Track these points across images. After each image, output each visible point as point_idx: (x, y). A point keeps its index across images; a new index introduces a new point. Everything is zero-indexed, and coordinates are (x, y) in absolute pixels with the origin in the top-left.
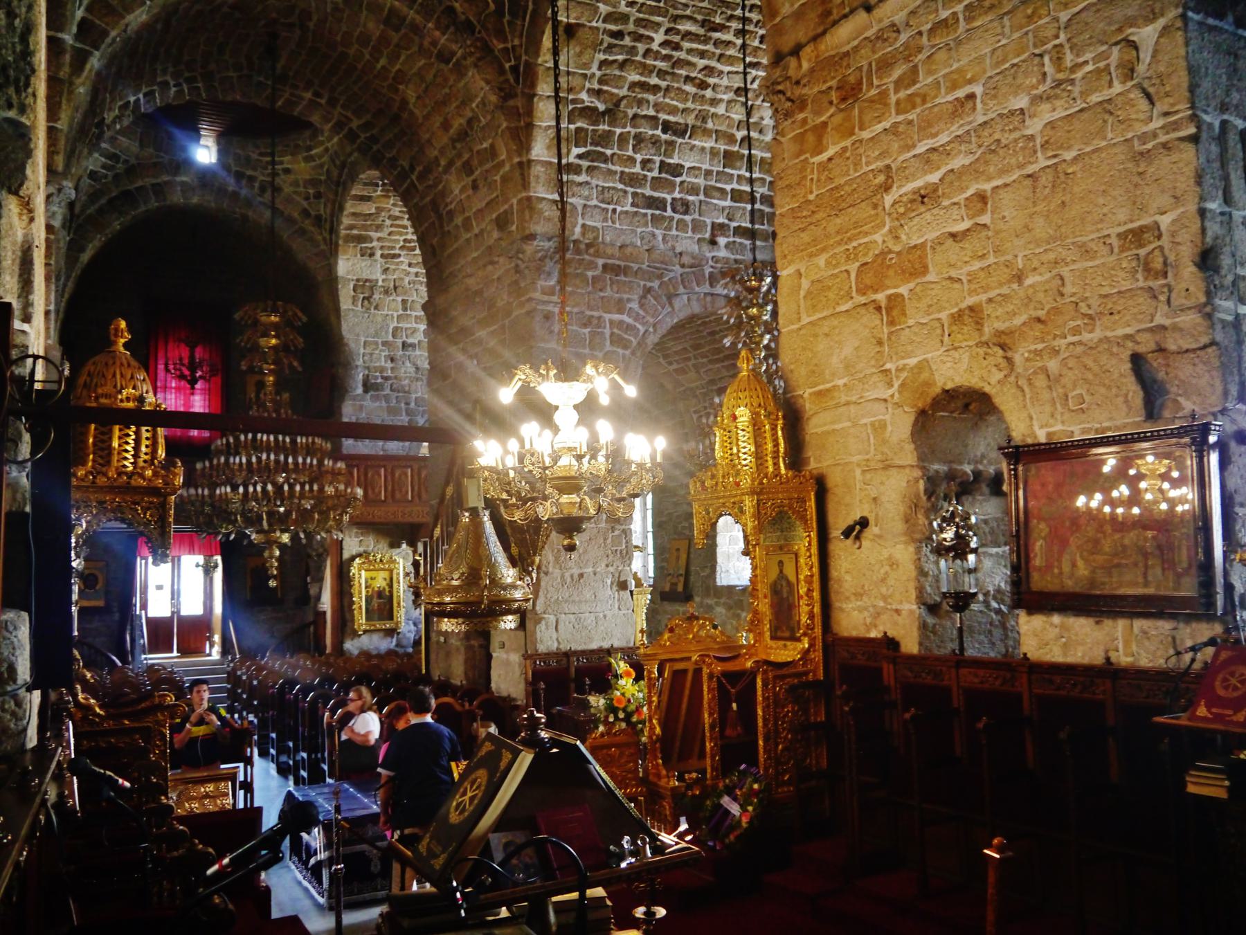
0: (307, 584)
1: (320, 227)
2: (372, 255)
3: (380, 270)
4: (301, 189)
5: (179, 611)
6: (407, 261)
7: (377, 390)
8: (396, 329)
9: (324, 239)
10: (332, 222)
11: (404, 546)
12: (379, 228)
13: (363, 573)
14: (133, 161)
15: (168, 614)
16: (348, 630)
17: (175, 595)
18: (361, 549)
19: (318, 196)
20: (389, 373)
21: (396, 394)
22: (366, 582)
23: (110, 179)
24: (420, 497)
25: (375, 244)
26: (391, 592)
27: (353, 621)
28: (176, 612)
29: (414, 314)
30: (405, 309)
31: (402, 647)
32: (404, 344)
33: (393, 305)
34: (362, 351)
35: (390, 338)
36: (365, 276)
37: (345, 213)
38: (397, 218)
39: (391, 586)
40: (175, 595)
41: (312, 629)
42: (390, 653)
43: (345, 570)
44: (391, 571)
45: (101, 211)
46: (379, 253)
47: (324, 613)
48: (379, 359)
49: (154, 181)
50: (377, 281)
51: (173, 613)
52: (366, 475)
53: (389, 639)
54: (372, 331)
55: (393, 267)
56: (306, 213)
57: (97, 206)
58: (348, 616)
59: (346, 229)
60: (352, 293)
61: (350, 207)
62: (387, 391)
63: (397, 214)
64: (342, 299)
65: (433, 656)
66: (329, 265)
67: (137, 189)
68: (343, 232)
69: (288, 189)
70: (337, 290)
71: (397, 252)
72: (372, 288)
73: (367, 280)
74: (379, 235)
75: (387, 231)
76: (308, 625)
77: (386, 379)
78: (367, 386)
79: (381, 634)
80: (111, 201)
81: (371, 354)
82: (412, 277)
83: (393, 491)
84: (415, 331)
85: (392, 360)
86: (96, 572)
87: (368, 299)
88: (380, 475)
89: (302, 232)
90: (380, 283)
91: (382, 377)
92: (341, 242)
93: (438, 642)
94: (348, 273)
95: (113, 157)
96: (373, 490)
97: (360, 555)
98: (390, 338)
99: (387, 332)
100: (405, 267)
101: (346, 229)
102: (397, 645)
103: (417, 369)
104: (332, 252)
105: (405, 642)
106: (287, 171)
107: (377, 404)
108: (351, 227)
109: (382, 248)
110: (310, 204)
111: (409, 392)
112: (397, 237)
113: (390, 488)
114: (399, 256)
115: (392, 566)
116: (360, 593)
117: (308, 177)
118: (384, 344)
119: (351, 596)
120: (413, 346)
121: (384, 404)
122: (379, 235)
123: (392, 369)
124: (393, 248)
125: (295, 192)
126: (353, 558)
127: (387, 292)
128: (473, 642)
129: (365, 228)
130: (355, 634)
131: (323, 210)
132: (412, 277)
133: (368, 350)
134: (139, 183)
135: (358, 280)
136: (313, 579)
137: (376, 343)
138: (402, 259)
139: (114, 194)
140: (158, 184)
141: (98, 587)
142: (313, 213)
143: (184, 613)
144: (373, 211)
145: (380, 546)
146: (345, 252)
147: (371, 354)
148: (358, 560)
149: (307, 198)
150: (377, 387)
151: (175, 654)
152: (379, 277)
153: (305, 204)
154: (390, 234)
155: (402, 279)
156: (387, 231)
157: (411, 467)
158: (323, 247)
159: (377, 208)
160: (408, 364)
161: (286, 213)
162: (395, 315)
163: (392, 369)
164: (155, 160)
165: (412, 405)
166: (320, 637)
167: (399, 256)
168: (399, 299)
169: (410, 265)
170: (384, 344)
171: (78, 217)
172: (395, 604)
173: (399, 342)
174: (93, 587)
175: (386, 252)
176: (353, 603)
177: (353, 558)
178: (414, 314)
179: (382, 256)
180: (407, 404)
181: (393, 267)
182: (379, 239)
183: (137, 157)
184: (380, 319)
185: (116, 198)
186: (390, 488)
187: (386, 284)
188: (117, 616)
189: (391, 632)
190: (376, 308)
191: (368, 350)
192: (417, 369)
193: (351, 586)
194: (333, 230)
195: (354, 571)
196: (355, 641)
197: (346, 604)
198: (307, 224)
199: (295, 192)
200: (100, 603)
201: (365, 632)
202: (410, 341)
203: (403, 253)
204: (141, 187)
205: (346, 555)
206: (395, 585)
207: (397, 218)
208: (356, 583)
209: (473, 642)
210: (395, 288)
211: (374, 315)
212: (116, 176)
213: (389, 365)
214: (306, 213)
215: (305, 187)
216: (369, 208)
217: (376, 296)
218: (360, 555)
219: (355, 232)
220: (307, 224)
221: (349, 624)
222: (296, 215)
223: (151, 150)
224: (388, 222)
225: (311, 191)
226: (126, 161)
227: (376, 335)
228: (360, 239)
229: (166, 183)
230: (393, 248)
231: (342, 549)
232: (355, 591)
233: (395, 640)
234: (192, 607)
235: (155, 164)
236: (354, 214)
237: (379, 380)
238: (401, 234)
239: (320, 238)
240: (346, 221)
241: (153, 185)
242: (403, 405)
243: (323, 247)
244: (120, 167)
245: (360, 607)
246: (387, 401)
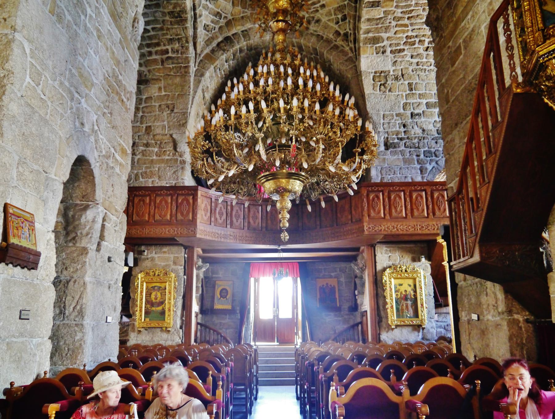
0: (355, 296)
1: (347, 41)
2: (383, 52)
3: (391, 63)
4: (333, 17)
5: (278, 316)
6: (410, 54)
7: (395, 147)
8: (405, 105)
9: (351, 49)
10: (355, 34)
11: (423, 260)
12: (387, 29)
13: (393, 280)
14: (230, 17)
15: (271, 317)
16: (384, 324)
17: (276, 306)
18: (390, 263)
19: (344, 18)
20: (403, 135)
21: (408, 150)
22: (395, 287)
23: (217, 29)
24: (434, 214)
25: (386, 43)
26: (415, 296)
27: (387, 317)
28: (276, 316)
29: (418, 92)
30: (411, 90)
31: (427, 340)
32: (412, 114)
33: (402, 88)
34: (382, 121)
35: (402, 111)
36: (380, 69)
37: (363, 19)
38: (400, 19)
39: (415, 291)
40: (276, 306)
41: (360, 326)
42: (418, 344)
43: (379, 278)
44: (415, 279)
45: (213, 51)
46: (389, 50)
47: (366, 311)
48: (395, 126)
49: (244, 29)
50: (389, 71)
51: (274, 316)
52: (389, 198)
53: (416, 333)
54: (388, 107)
55: (400, 60)
56: (338, 33)
57: (210, 48)
58: (382, 313)
59: (365, 33)
60: (373, 82)
61: (366, 13)
62: (403, 148)
63: (400, 15)
64: (365, 87)
65: (464, 338)
66: (355, 66)
67: (233, 35)
68: (362, 36)
69: (324, 19)
70: (362, 80)
71: (402, 47)
72: (386, 77)
73: (381, 72)
74: (388, 35)
75: (393, 30)
76: (357, 325)
77: (401, 139)
78: (387, 146)
79: (410, 329)
80: (218, 44)
81: (389, 123)
82: (414, 66)
83: (412, 210)
84: (419, 104)
85: (404, 126)
86: (226, 287)
87: (384, 85)
88: (400, 198)
89: (336, 47)
90: (392, 73)
91: (398, 139)
92: (361, 45)
93: (469, 321)
94: (368, 68)
95: (218, 14)
96: (396, 208)
97: (390, 267)
98: (402, 111)
99: (399, 107)
100: (408, 58)
101: (365, 33)
102: (423, 339)
103: (424, 130)
104: (356, 52)
105: (429, 336)
106: (323, 6)
107: (396, 157)
108: (368, 32)
109: (391, 45)
110: (339, 26)
111: (419, 147)
112: (401, 35)
113: (409, 207)
114: (404, 50)
115: (415, 275)
116: (391, 296)
117: (336, 6)
118: (397, 115)
119: (385, 297)
120: (419, 115)
121: (400, 157)
122: (388, 35)
123: (405, 132)
124: (398, 44)
125: (329, 20)
126: (384, 270)
127: (396, 78)
128: (516, 316)
129: (377, 30)
130: (389, 328)
131: (347, 28)
132: (414, 66)
133: (386, 120)
134: (234, 31)
135: (376, 73)
136: (359, 292)
137: (392, 115)
138: (405, 53)
139: (220, 39)
140: (246, 31)
141: (227, 297)
142: (342, 33)
143: (281, 316)
144: (382, 15)
145: (405, 260)
146: (365, 51)
147: (389, 123)
148: (388, 269)
149: (337, 23)
150: (395, 146)
151: (276, 343)
152: (389, 67)
153: (336, 27)
154: (395, 33)
155: (408, 68)
156: (393, 30)
157: (425, 190)
158: (351, 55)
159: (385, 12)
160: (416, 127)
161: (325, 37)
162: (404, 94)
163: (405, 132)
164: (242, 15)
165: (422, 156)
166: (364, 334)
167: (404, 50)
168: (406, 82)
169: (412, 57)
170: (397, 115)
171: (200, 55)
172: (419, 305)
173: (408, 113)
174: (225, 297)
175: (394, 48)
176: (385, 303)
177: (384, 270)
178: (418, 92)
179: (391, 52)
180: (418, 156)
181: (400, 60)
182: (388, 38)
183: (232, 15)
184: (393, 98)
185: (222, 42)
186: (409, 207)
187: (396, 73)
188: (239, 316)
189: (418, 327)
190: (390, 91)
191: (386, 120)
192: (424, 130)
193: (384, 291)
194: (355, 40)
195: (386, 278)
196: (390, 332)
197: (381, 303)
198: (339, 42)
199: (329, 20)
200: (229, 307)
201: (397, 326)
202: (416, 112)
203: (406, 48)
204: (235, 34)
205: (379, 267)
206: (418, 290)
207: (400, 19)
208: (388, 288)
209: (516, 316)
210: (403, 75)
211: (389, 96)
212: (220, 28)
213: (402, 129)
214: (338, 33)
215: (335, 14)
216: (378, 13)
217: (389, 82)
218: (390, 267)
219: (371, 35)
220: (339, 42)
221: (384, 320)
222: (331, 36)
223: (240, 8)
224: (394, 23)
225: (340, 16)
226: (225, 17)
227: (391, 109)
228: (375, 40)
229: (250, 29)
230: (398, 44)
231: (375, 262)
232: (387, 293)
233: (421, 334)
234: (286, 313)
235: (242, 17)
236: (369, 20)
237: (396, 141)
238: (404, 32)
239: (347, 48)
240: (364, 26)
241: (242, 31)
242: (415, 157)
243: (351, 55)
244: (223, 22)
245: (392, 307)
246: (403, 155)
